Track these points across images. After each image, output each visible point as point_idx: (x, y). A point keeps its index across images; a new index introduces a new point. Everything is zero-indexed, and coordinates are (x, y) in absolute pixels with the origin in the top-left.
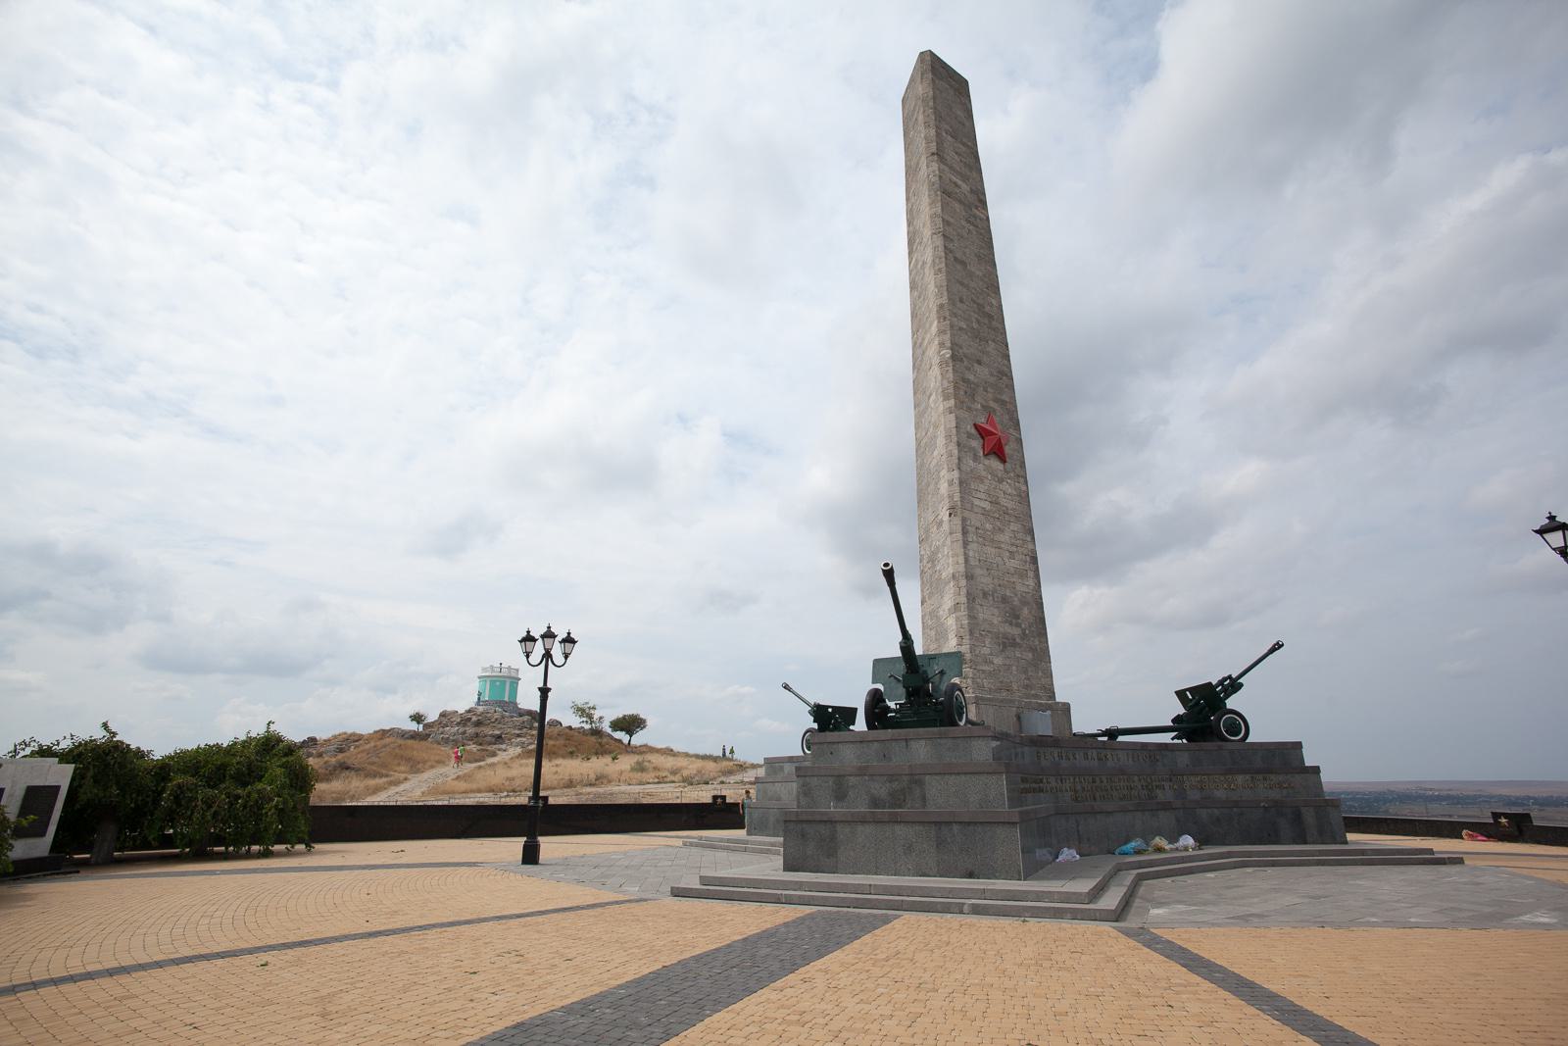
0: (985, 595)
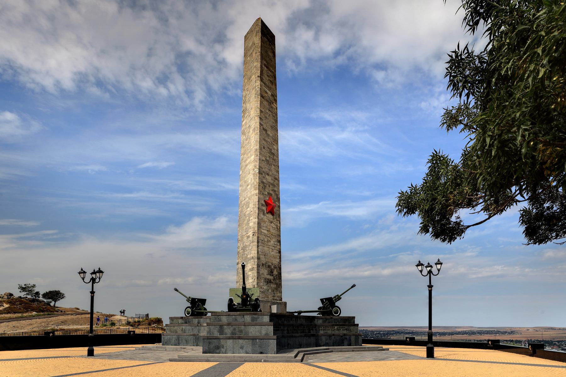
0: (263, 265)
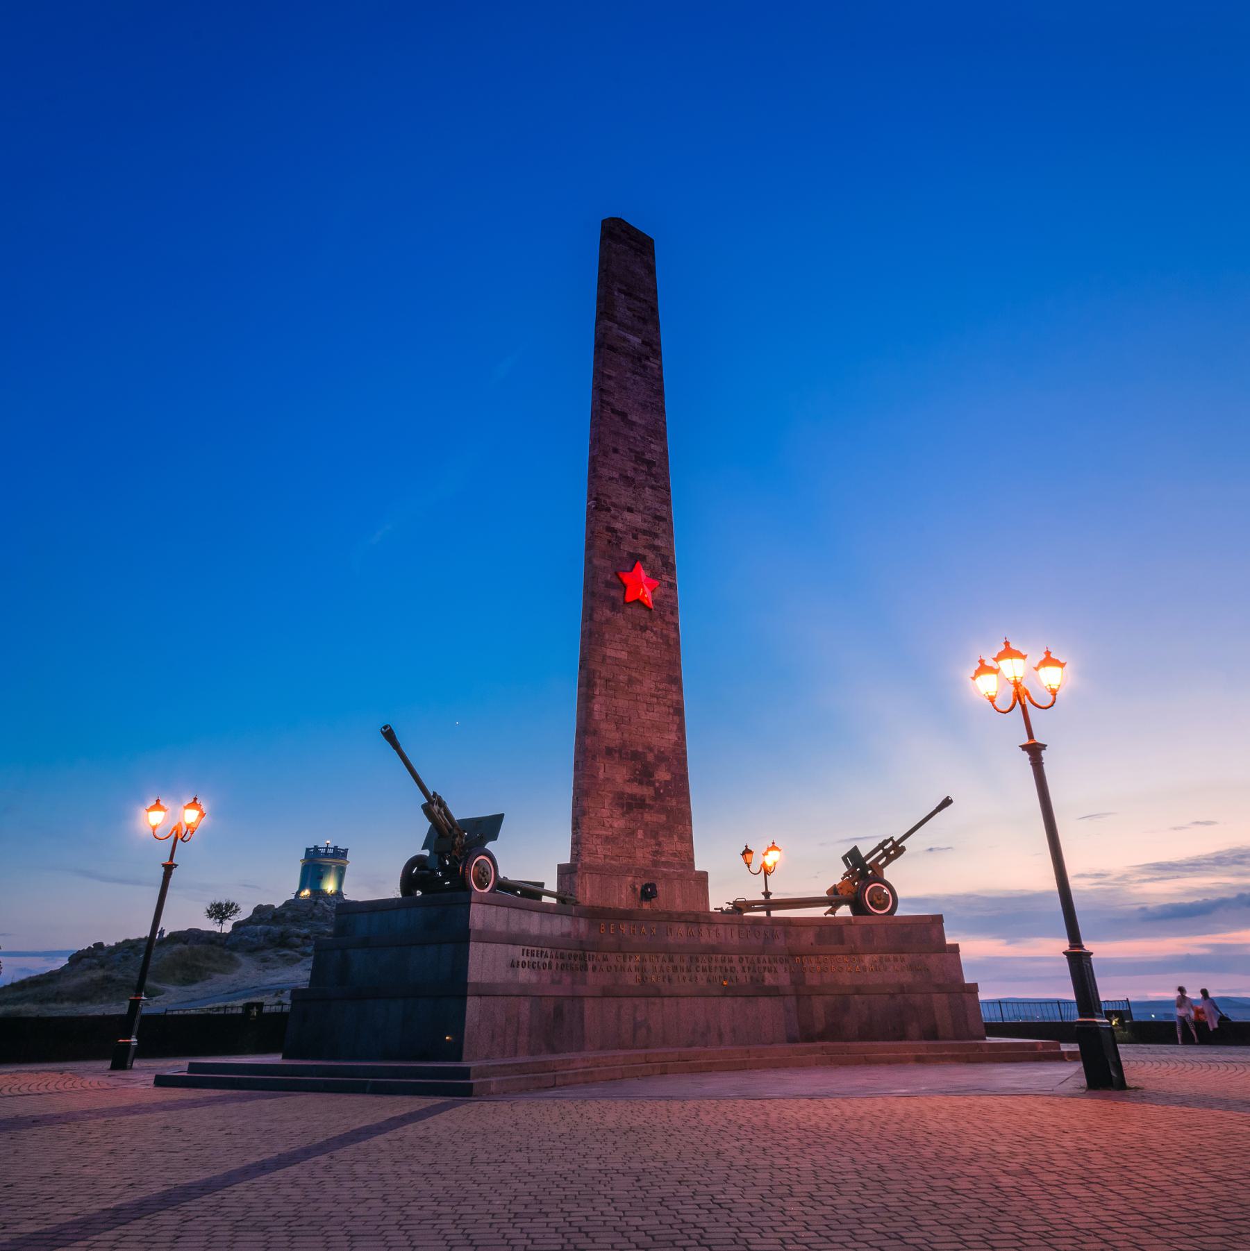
0: (609, 752)
